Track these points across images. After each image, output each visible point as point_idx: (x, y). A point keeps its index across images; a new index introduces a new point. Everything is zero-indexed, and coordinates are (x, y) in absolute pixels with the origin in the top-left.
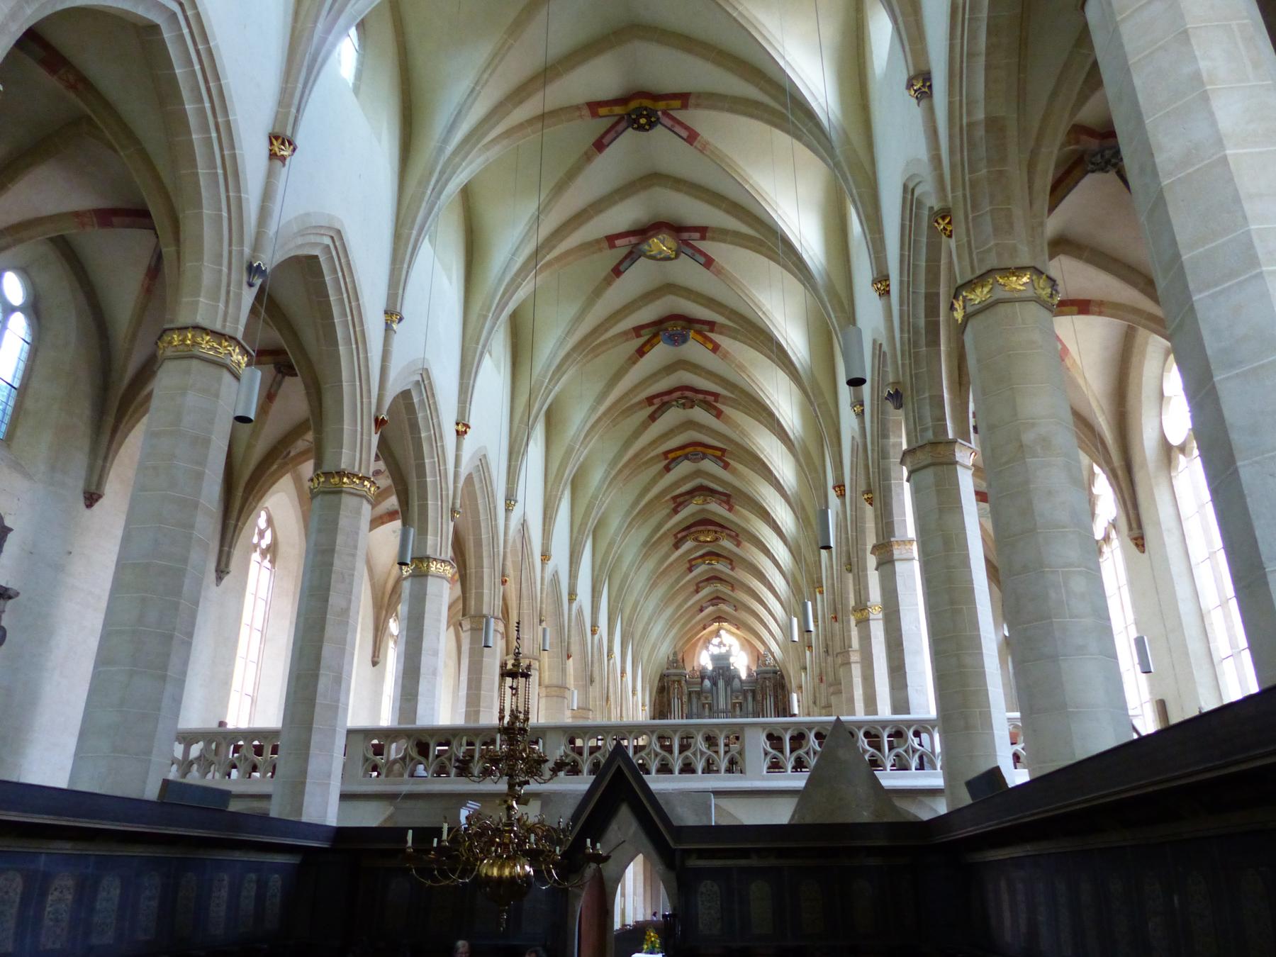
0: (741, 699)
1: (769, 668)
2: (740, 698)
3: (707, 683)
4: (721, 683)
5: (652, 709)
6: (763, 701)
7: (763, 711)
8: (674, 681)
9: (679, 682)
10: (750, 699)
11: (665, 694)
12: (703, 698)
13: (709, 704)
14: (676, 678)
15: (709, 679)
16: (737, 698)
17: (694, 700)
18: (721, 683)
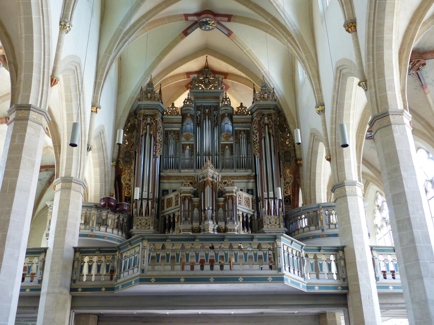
0: (231, 140)
1: (269, 102)
2: (231, 139)
3: (189, 125)
4: (207, 124)
5: (116, 151)
6: (261, 140)
7: (260, 152)
8: (147, 116)
9: (153, 117)
10: (243, 141)
11: (135, 133)
12: (183, 139)
13: (191, 146)
14: (148, 112)
15: (192, 116)
16: (227, 138)
17: (172, 141)
18: (207, 124)
